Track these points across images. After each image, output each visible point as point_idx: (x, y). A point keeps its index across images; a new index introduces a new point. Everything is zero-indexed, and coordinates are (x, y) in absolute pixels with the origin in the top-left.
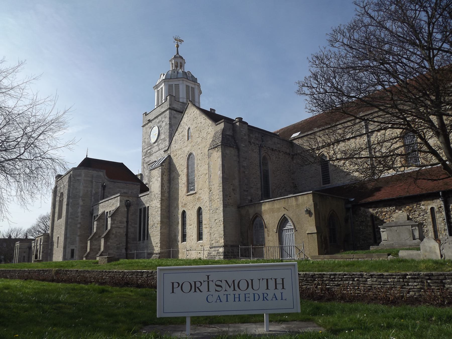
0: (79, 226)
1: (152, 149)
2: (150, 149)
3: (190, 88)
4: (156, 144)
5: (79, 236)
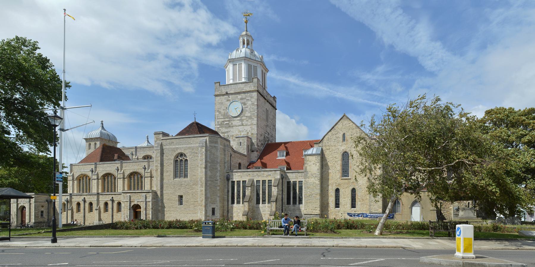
0: (218, 188)
1: (232, 122)
2: (229, 121)
3: (252, 66)
4: (239, 118)
5: (219, 197)
